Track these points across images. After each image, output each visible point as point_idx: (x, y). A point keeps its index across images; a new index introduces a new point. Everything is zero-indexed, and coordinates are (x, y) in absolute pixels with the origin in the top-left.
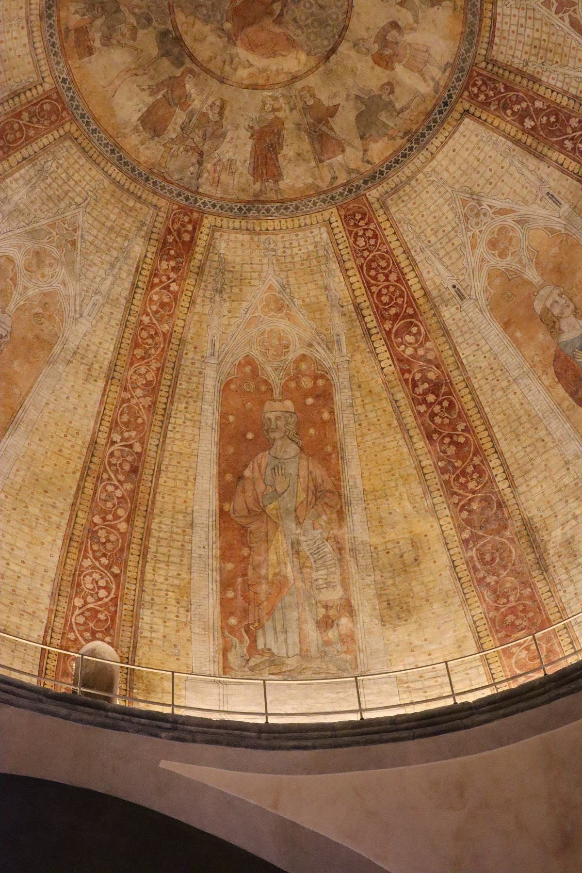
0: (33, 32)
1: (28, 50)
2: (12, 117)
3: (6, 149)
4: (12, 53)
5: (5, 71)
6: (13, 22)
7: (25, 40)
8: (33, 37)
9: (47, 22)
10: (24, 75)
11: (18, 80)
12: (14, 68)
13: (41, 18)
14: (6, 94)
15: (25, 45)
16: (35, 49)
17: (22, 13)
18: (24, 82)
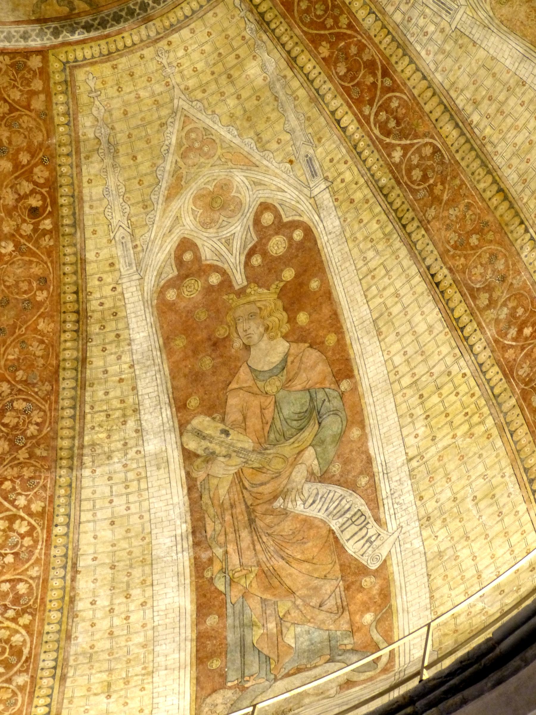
0: (172, 25)
1: (199, 23)
2: (293, 17)
3: (337, 12)
4: (207, 48)
5: (234, 50)
6: (165, 62)
7: (185, 32)
8: (178, 21)
9: (153, 8)
10: (233, 17)
11: (242, 25)
12: (227, 37)
13: (147, 20)
14: (265, 37)
15: (193, 31)
16: (193, 12)
17: (148, 52)
18: (242, 14)
